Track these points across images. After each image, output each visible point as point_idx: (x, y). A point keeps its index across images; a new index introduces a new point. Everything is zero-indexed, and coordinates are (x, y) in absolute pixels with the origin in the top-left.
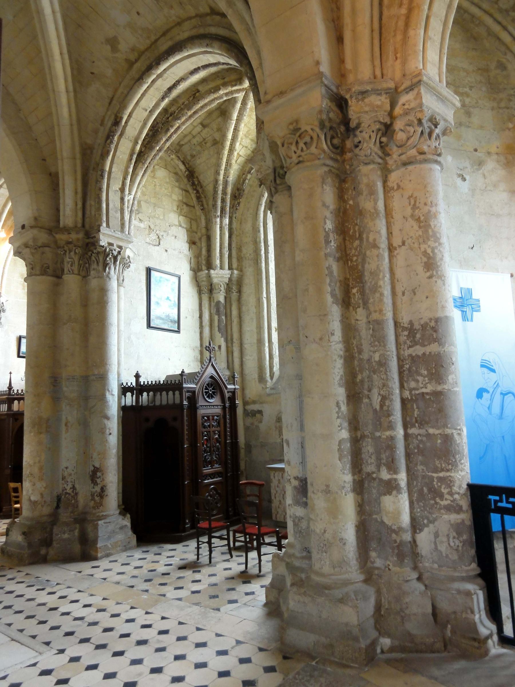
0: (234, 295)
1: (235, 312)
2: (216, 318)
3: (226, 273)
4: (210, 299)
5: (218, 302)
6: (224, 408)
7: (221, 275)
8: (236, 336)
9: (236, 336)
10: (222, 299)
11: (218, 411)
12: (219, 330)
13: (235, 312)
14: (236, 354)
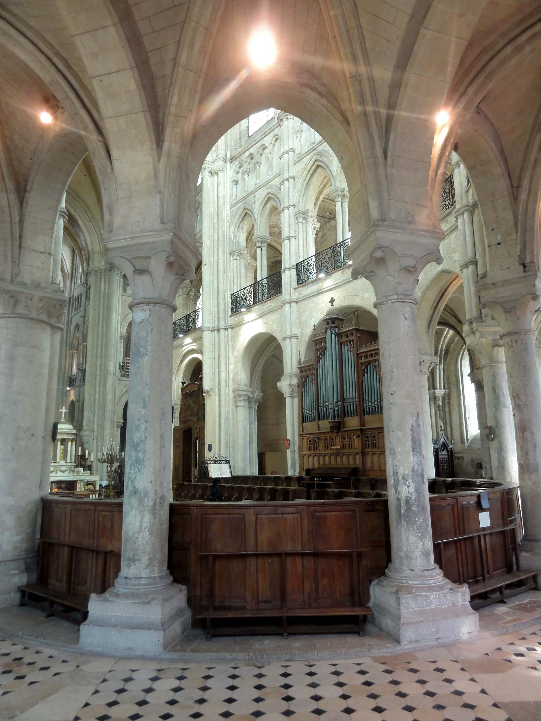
0: (447, 401)
1: (447, 410)
2: (438, 412)
3: (443, 391)
4: (435, 403)
5: (439, 405)
6: (448, 455)
7: (440, 392)
8: (448, 421)
9: (448, 421)
10: (441, 404)
11: (446, 456)
12: (440, 418)
13: (447, 410)
14: (449, 429)
